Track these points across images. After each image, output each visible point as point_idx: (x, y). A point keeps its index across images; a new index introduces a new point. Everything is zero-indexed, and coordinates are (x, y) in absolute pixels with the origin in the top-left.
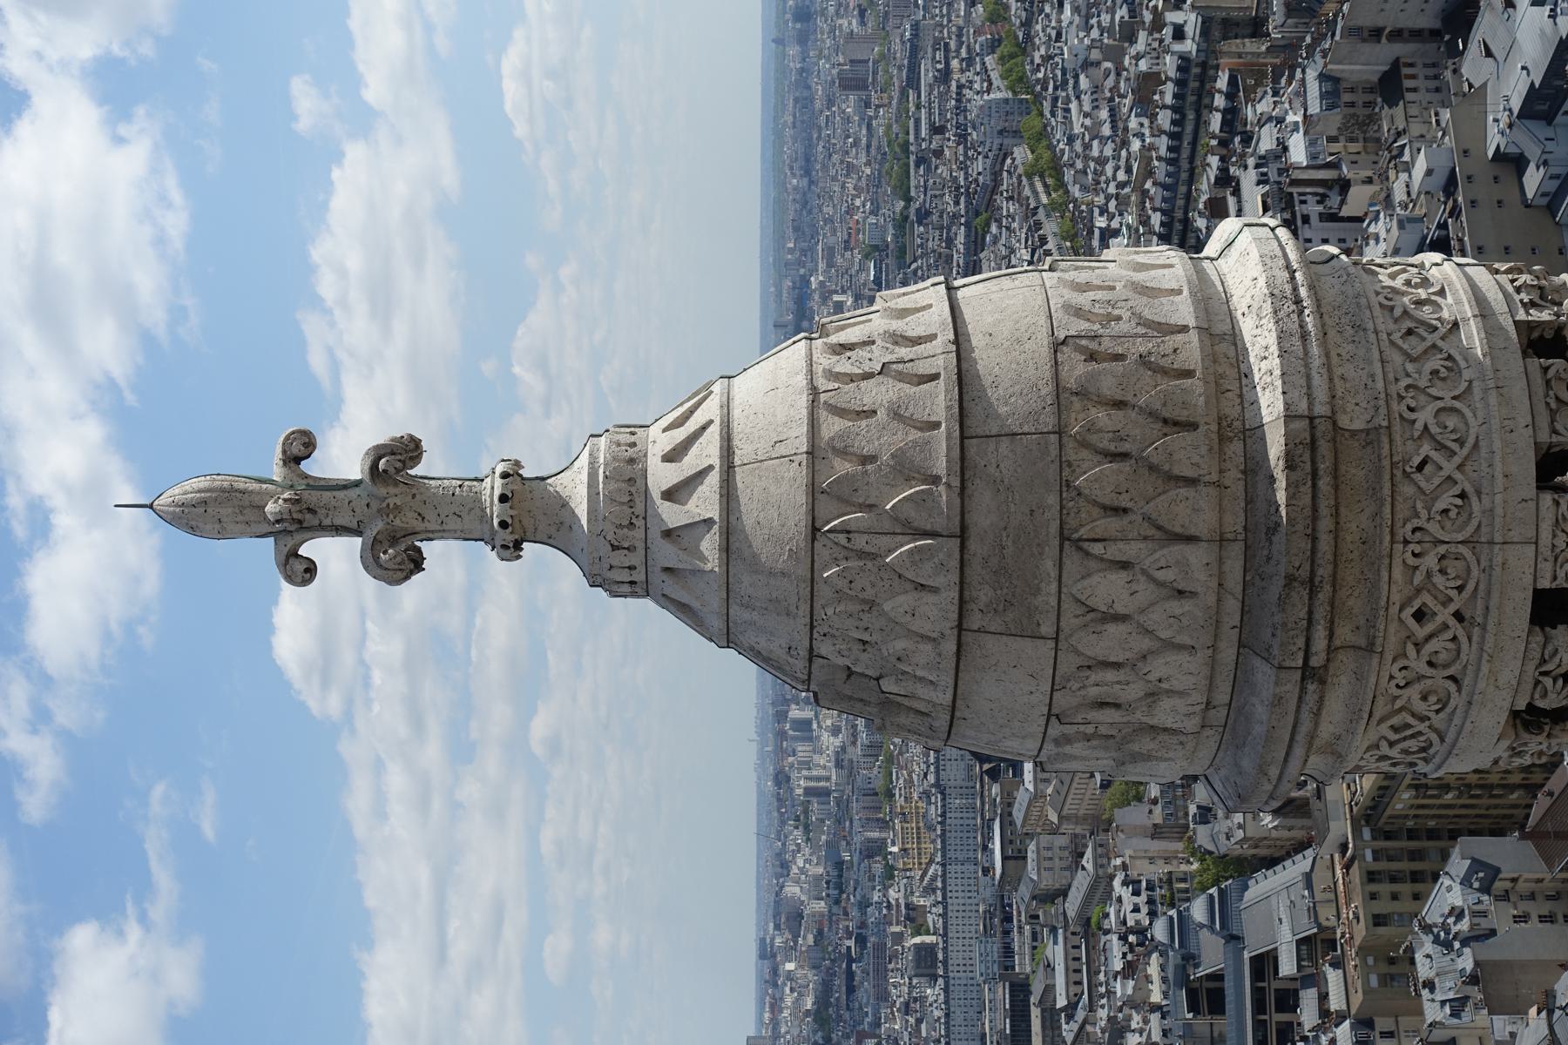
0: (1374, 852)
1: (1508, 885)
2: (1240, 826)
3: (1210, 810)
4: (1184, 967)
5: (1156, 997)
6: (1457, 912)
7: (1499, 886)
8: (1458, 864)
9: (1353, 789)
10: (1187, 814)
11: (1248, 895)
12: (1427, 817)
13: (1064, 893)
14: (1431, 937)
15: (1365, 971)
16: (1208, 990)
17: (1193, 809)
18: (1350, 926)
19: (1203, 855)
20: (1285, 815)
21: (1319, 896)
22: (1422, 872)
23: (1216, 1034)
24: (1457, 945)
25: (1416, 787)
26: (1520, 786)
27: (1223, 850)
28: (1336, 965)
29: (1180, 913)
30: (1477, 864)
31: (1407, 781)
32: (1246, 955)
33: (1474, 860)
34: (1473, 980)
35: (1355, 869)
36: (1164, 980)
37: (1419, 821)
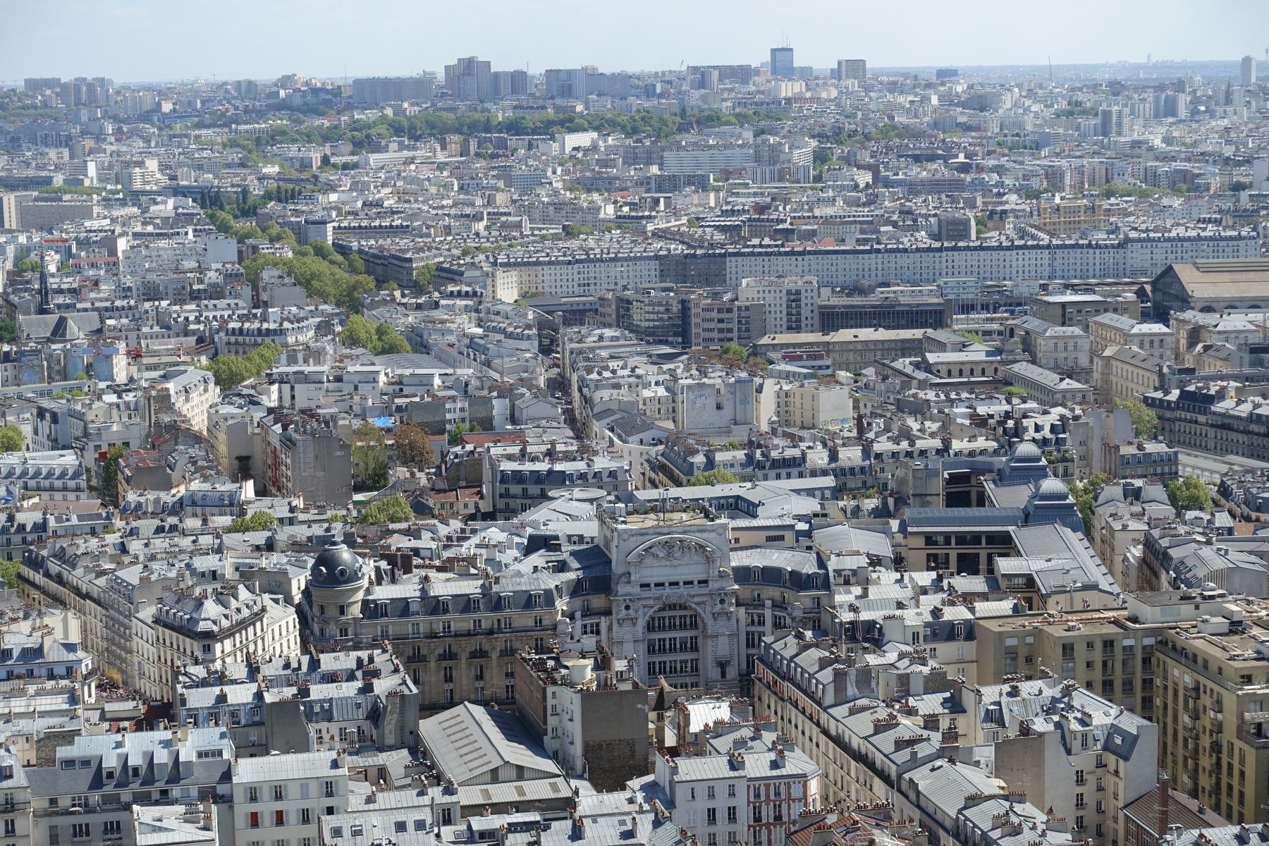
0: (1131, 647)
1: (1112, 767)
2: (1125, 527)
3: (1137, 499)
4: (991, 471)
5: (956, 445)
6: (1086, 719)
7: (1111, 759)
8: (1132, 723)
9: (1192, 630)
10: (1133, 477)
11: (1068, 531)
12: (1165, 697)
13: (1033, 362)
14: (1059, 696)
15: (1021, 635)
16: (968, 493)
17: (1138, 483)
18: (1061, 622)
19: (1094, 489)
20: (1140, 569)
21: (1079, 596)
22: (1112, 690)
23: (929, 498)
24: (1056, 718)
25: (1197, 689)
26: (1196, 785)
27: (1099, 510)
28: (1016, 608)
29: (1044, 468)
30: (1132, 740)
31: (1203, 680)
32: (1011, 529)
33: (1136, 738)
34: (1025, 730)
35: (1114, 629)
36: (972, 454)
37: (1161, 691)
